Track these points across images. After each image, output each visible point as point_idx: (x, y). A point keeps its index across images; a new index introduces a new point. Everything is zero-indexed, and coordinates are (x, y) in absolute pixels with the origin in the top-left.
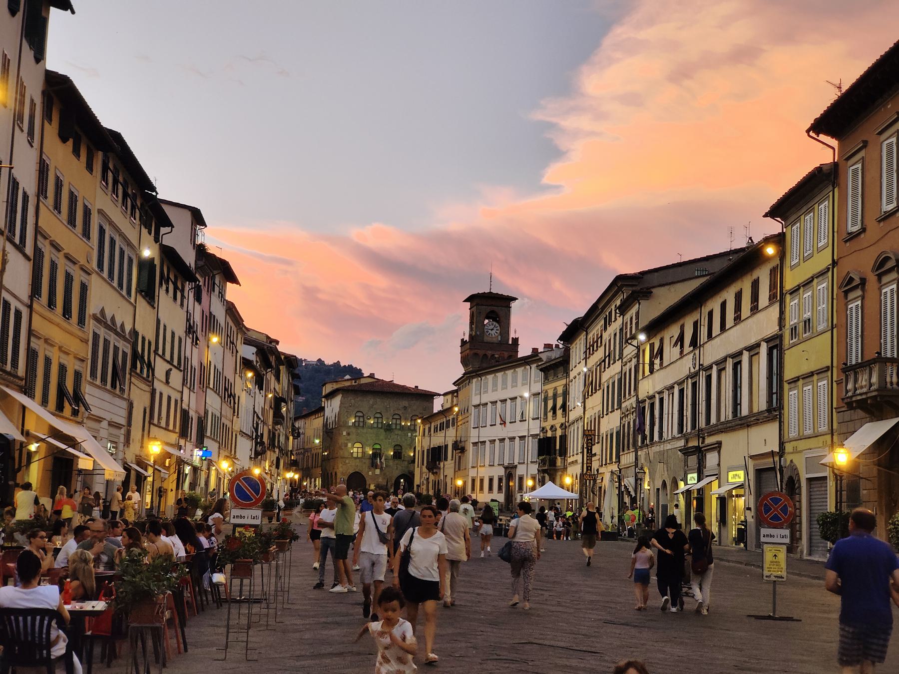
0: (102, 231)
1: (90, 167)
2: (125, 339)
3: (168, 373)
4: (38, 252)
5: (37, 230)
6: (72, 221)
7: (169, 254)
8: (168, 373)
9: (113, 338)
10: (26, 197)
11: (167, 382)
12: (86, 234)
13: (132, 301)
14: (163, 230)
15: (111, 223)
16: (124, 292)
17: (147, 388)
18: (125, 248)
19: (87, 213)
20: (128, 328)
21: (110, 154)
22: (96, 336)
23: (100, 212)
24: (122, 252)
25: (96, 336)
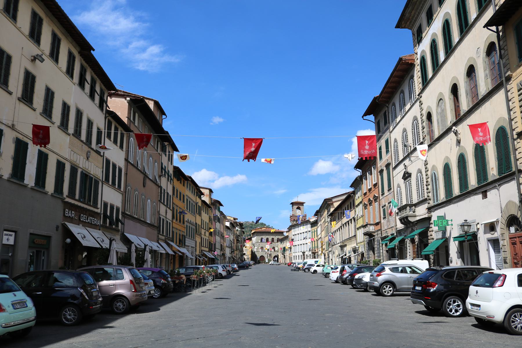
0: (187, 200)
1: (184, 185)
2: (193, 225)
3: (205, 233)
4: (173, 208)
5: (173, 203)
6: (180, 199)
7: (204, 202)
8: (205, 233)
9: (191, 225)
10: (170, 196)
11: (205, 235)
12: (184, 202)
13: (195, 216)
14: (202, 196)
15: (189, 197)
16: (193, 214)
17: (200, 237)
18: (193, 203)
19: (184, 196)
20: (194, 223)
21: (188, 181)
22: (187, 226)
23: (186, 195)
24: (192, 204)
25: (187, 226)
